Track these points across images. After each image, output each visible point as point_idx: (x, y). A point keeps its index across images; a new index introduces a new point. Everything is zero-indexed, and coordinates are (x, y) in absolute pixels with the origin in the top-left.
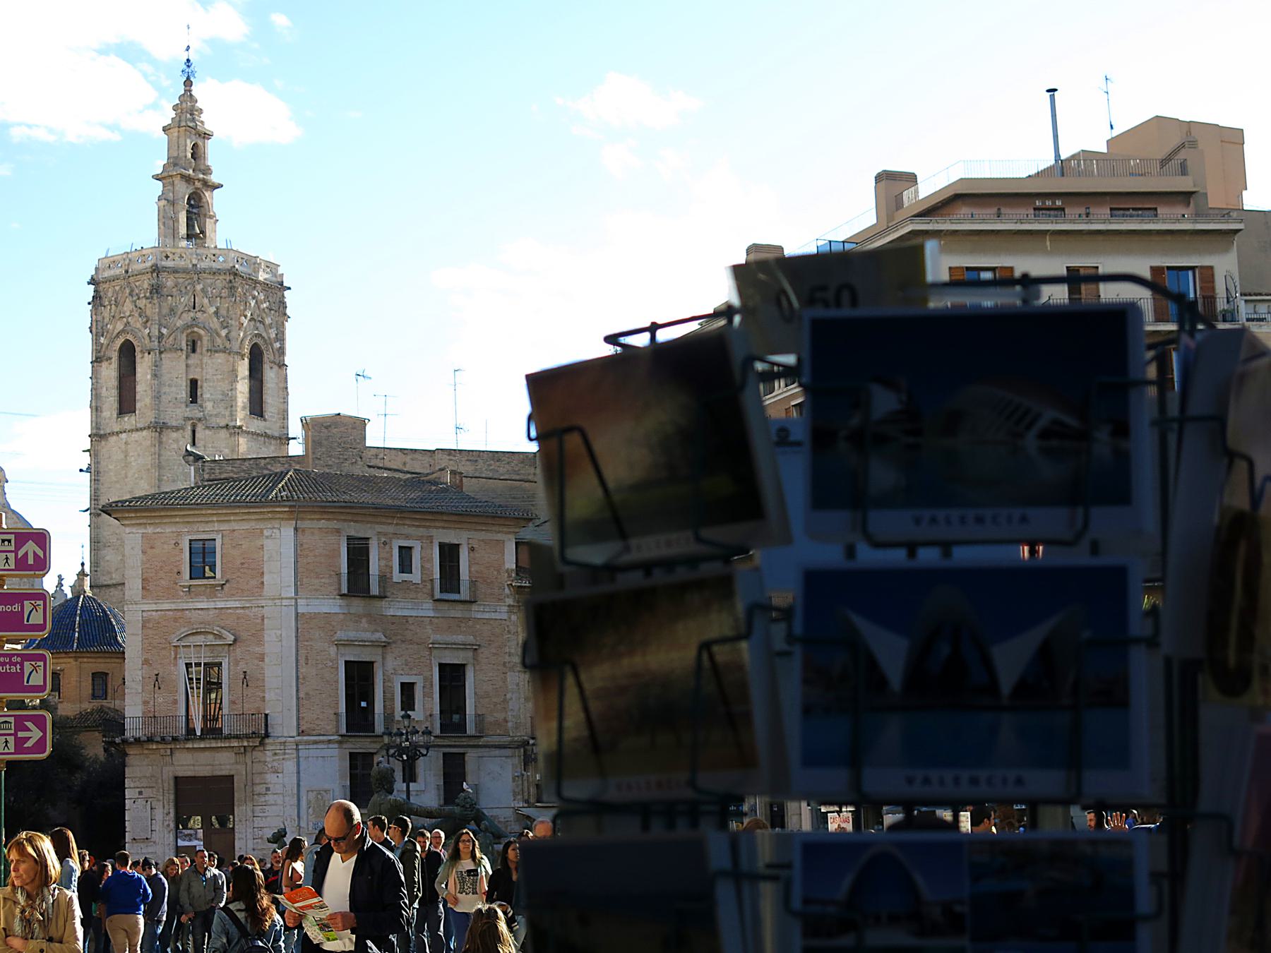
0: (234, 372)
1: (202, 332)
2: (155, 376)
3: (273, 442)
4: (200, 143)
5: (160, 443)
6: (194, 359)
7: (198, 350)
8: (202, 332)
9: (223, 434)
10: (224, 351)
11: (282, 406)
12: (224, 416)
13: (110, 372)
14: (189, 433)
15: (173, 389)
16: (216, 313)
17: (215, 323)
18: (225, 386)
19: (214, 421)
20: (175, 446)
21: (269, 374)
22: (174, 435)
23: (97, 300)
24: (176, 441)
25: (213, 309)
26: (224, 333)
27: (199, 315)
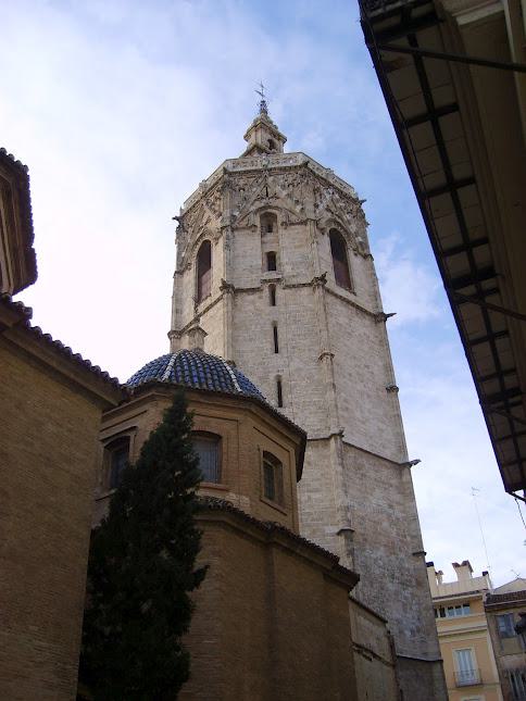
1: (274, 211)
2: (227, 246)
3: (367, 317)
4: (276, 141)
5: (234, 305)
6: (269, 237)
8: (274, 211)
9: (306, 291)
13: (190, 277)
14: (266, 292)
16: (289, 195)
17: (289, 203)
19: (294, 281)
20: (251, 307)
21: (355, 262)
22: (251, 297)
23: (181, 230)
24: (253, 302)
25: (285, 193)
26: (298, 208)
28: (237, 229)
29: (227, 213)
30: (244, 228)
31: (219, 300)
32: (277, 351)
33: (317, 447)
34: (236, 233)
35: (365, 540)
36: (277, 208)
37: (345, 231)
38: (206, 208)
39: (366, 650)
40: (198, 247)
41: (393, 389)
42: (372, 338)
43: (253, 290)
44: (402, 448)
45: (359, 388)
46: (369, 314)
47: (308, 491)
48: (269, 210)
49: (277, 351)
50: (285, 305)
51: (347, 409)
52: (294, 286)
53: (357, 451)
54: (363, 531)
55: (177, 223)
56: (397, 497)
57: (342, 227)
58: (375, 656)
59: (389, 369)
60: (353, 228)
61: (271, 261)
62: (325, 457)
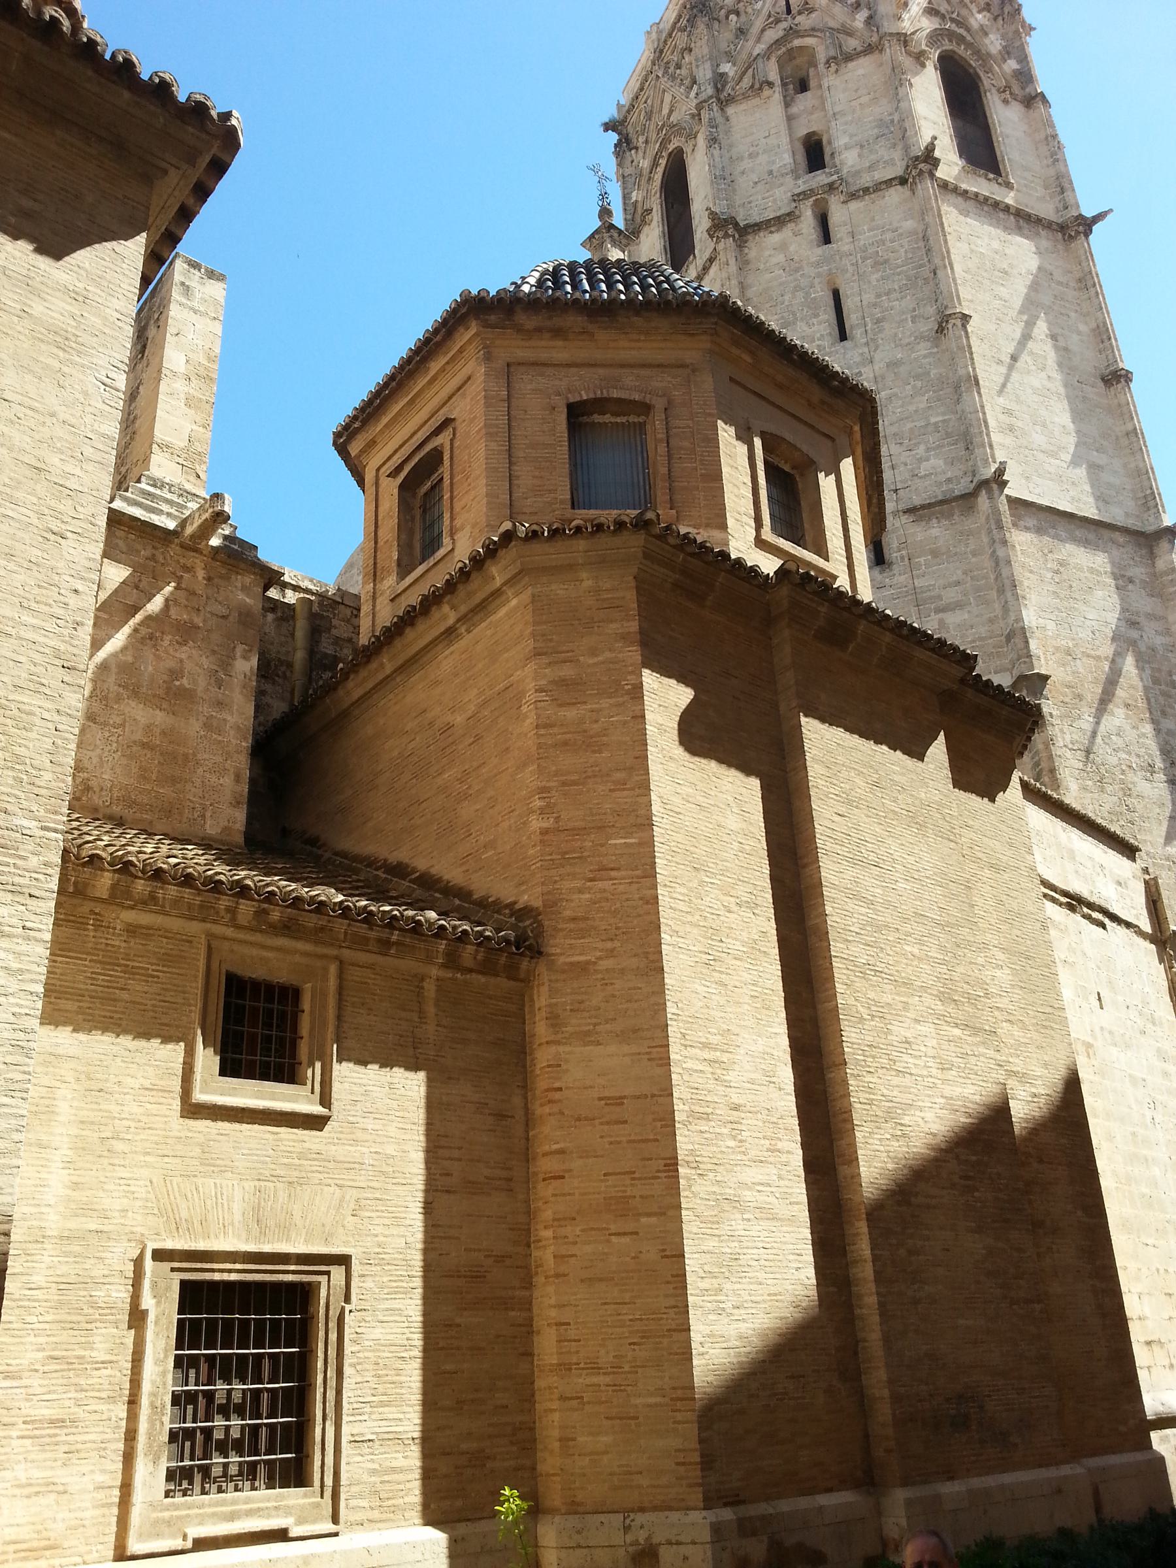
0: (896, 83)
1: (809, 41)
2: (713, 141)
3: (1043, 233)
6: (804, 102)
7: (813, 83)
8: (809, 41)
9: (895, 195)
10: (869, 49)
11: (1052, 172)
12: (891, 162)
14: (808, 221)
15: (763, 159)
18: (883, 109)
19: (866, 180)
20: (780, 258)
22: (775, 238)
23: (624, 146)
24: (783, 247)
27: (799, 19)
28: (731, 100)
29: (704, 73)
30: (745, 97)
31: (711, 260)
32: (843, 337)
33: (950, 516)
34: (731, 110)
35: (1080, 697)
36: (813, 31)
37: (977, 52)
38: (664, 82)
39: (1091, 906)
40: (660, 170)
41: (1116, 378)
42: (1058, 275)
43: (779, 222)
44: (1149, 500)
45: (1036, 383)
46: (1048, 225)
47: (938, 610)
48: (797, 42)
49: (843, 337)
50: (853, 235)
51: (1011, 429)
52: (866, 190)
53: (1042, 515)
54: (1069, 678)
55: (613, 137)
56: (1144, 603)
57: (969, 45)
58: (1114, 918)
59: (1103, 336)
60: (994, 43)
61: (815, 153)
62: (970, 533)
